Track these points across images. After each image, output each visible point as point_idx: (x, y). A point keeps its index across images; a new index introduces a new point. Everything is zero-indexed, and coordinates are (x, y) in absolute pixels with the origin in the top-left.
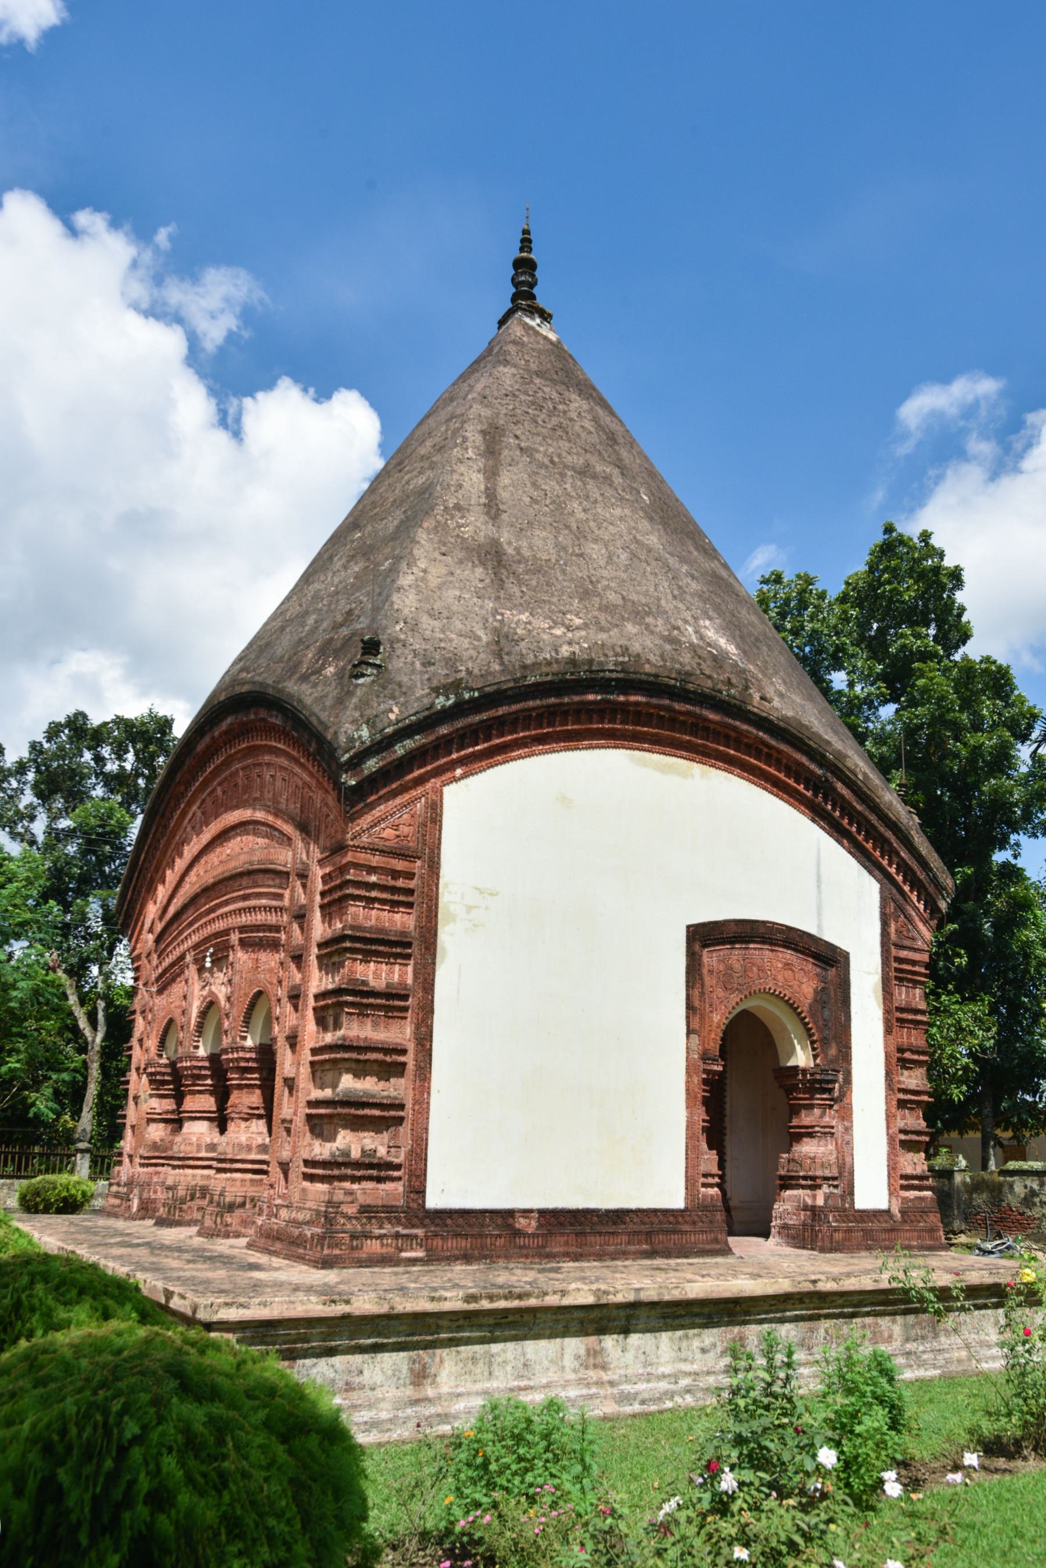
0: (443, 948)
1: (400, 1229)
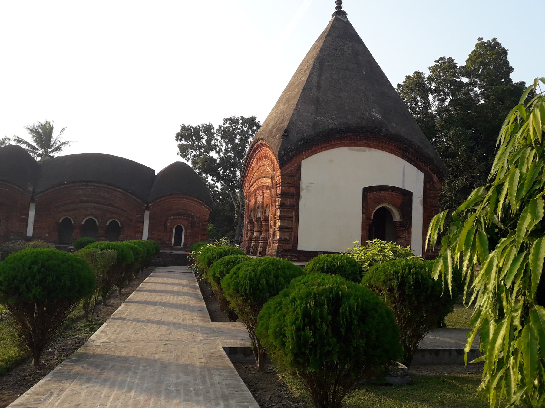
0: (301, 196)
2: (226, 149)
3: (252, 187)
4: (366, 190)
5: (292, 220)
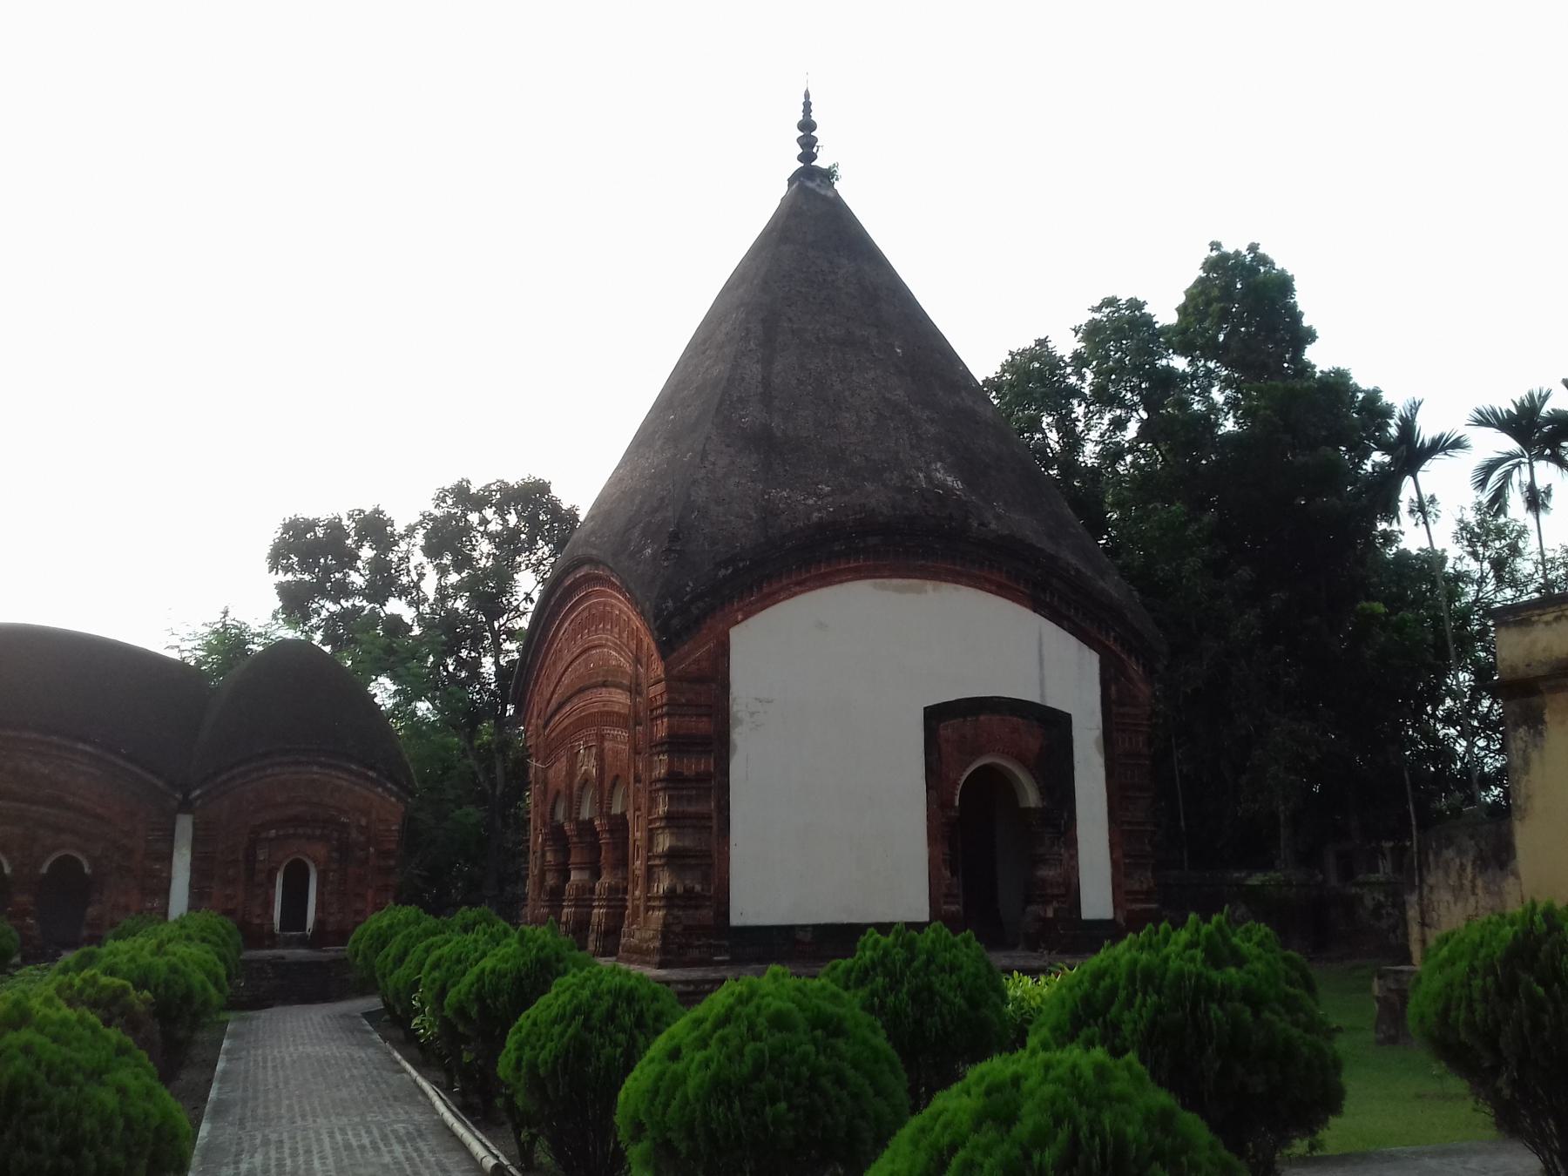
1: (712, 941)
2: (441, 590)
3: (557, 718)
4: (935, 716)
5: (710, 824)
